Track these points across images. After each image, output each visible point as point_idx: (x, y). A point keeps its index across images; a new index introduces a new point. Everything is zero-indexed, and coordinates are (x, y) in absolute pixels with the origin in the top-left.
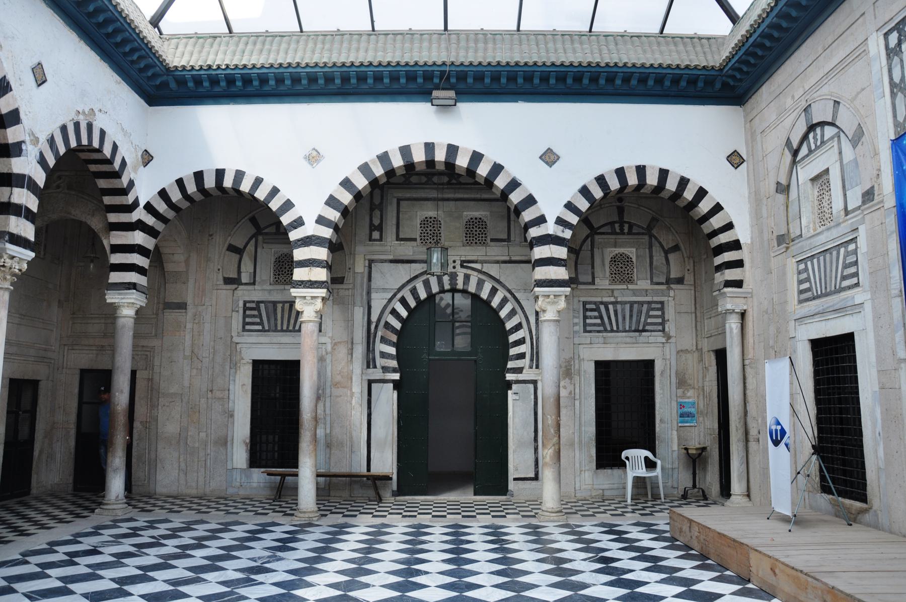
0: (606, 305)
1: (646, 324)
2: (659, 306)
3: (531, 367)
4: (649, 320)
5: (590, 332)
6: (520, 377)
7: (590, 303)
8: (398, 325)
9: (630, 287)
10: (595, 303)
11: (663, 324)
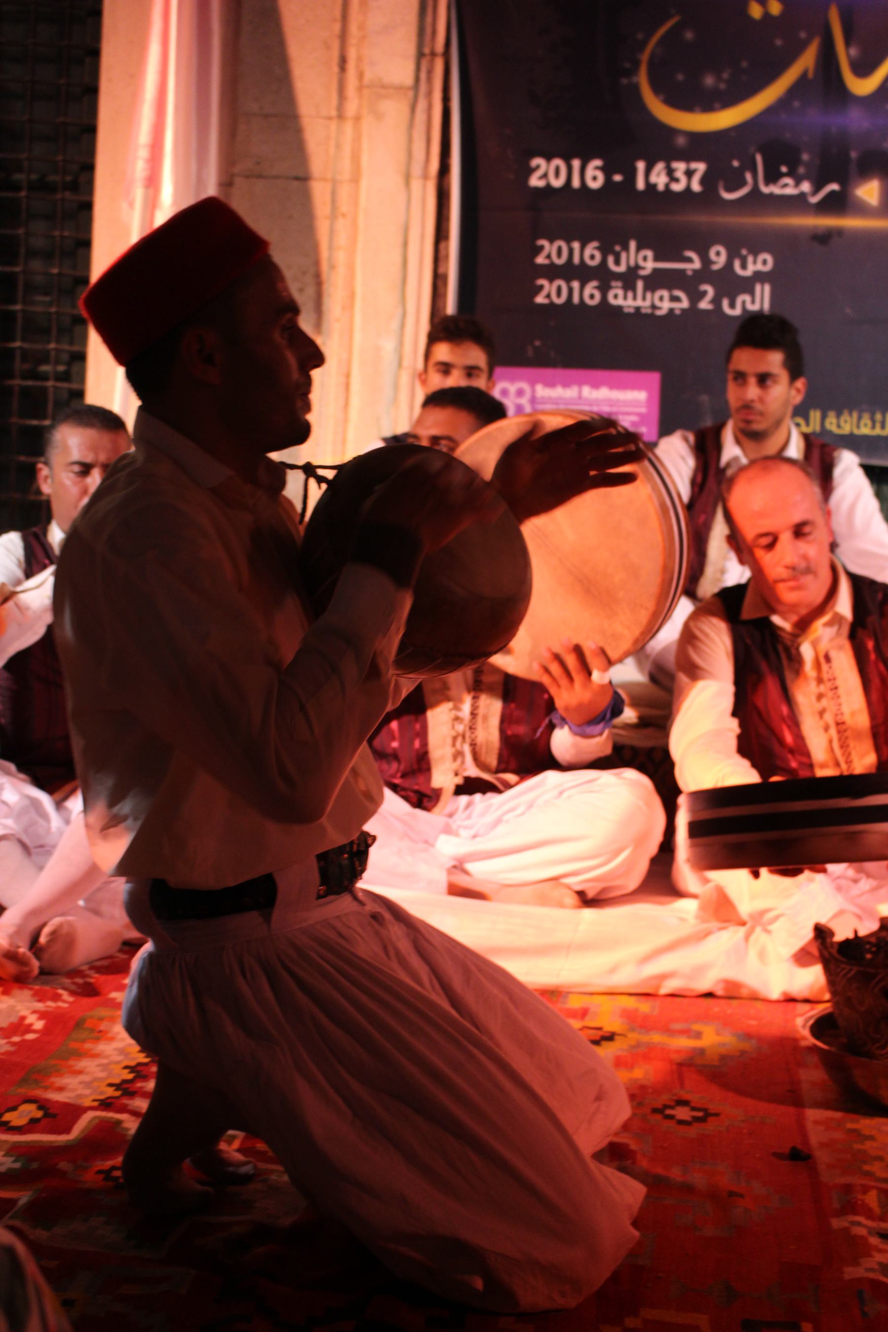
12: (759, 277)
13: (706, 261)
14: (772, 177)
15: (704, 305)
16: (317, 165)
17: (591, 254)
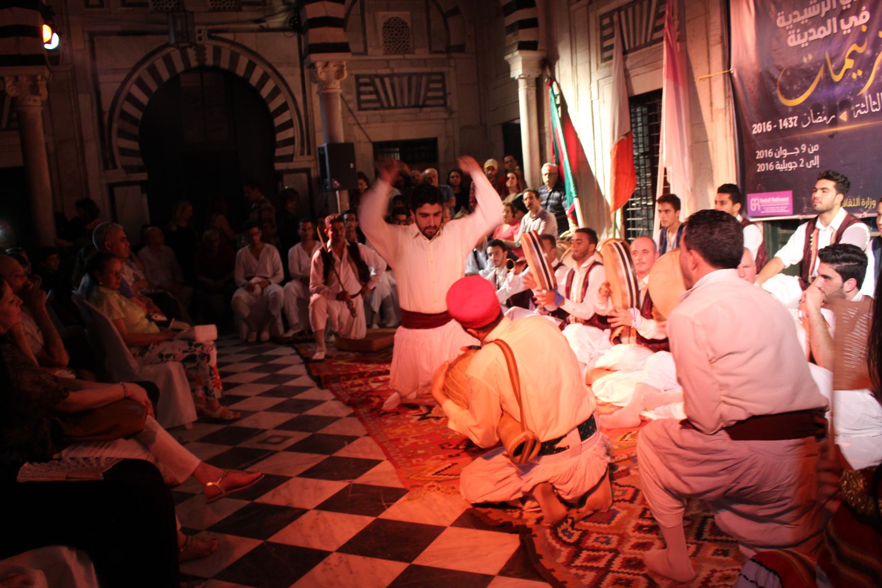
0: (381, 78)
1: (426, 98)
2: (439, 77)
3: (302, 154)
4: (430, 94)
5: (366, 109)
6: (291, 166)
7: (364, 76)
8: (137, 114)
9: (407, 56)
10: (369, 76)
11: (444, 97)
12: (815, 153)
13: (801, 151)
14: (816, 117)
15: (801, 166)
16: (709, 137)
17: (769, 153)
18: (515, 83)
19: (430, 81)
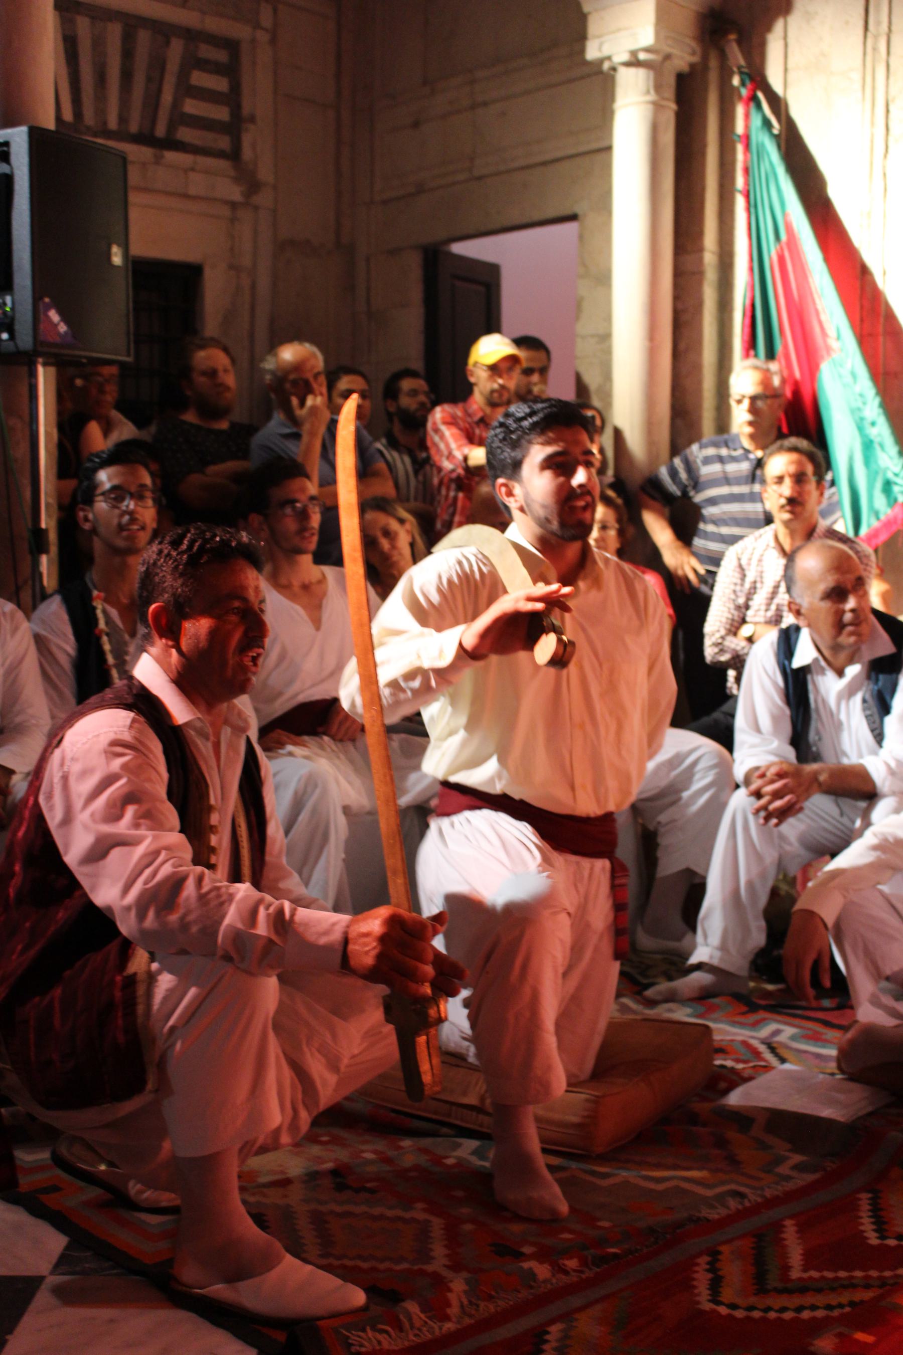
1: (179, 119)
4: (191, 107)
11: (234, 128)
18: (601, 80)
19: (192, 62)
